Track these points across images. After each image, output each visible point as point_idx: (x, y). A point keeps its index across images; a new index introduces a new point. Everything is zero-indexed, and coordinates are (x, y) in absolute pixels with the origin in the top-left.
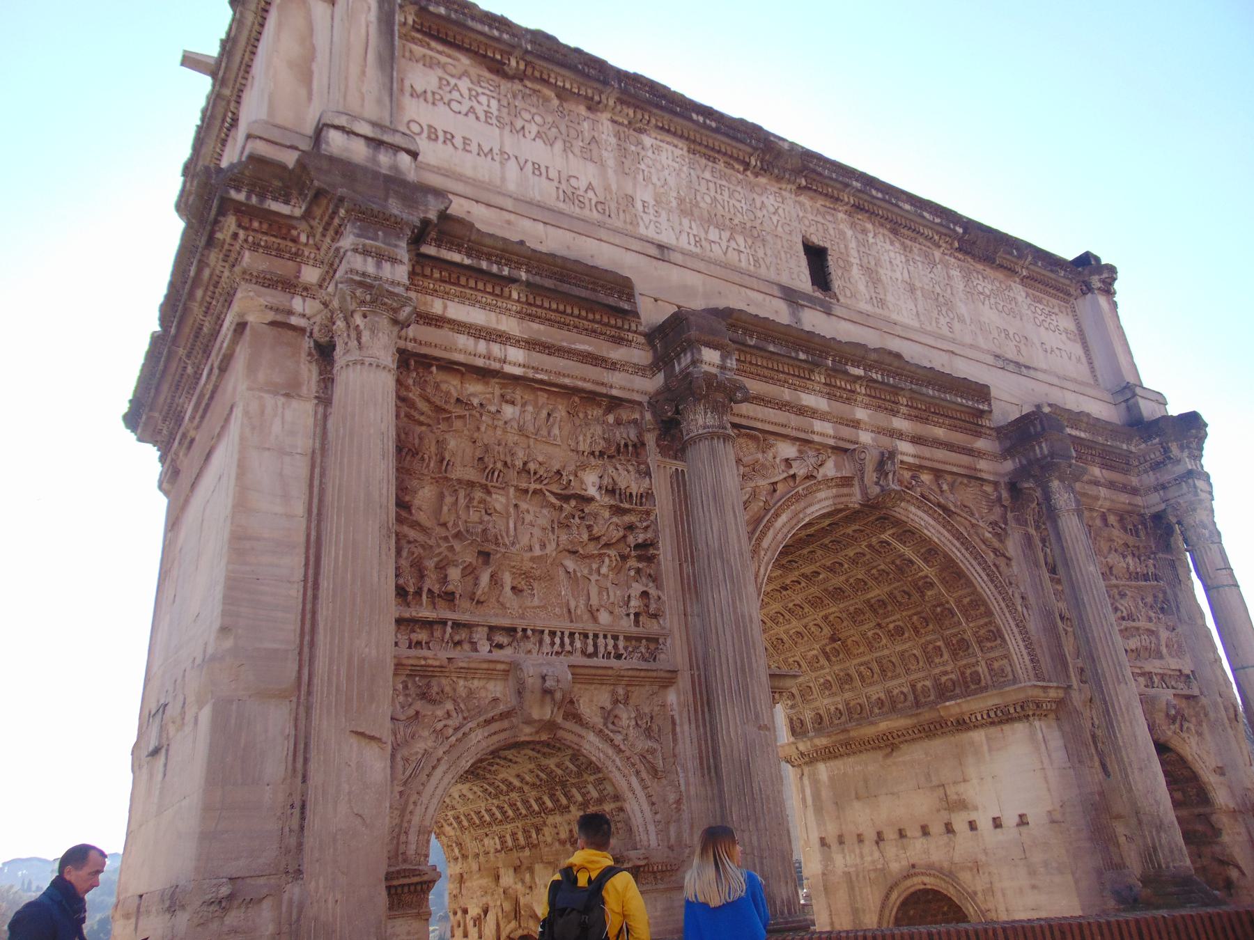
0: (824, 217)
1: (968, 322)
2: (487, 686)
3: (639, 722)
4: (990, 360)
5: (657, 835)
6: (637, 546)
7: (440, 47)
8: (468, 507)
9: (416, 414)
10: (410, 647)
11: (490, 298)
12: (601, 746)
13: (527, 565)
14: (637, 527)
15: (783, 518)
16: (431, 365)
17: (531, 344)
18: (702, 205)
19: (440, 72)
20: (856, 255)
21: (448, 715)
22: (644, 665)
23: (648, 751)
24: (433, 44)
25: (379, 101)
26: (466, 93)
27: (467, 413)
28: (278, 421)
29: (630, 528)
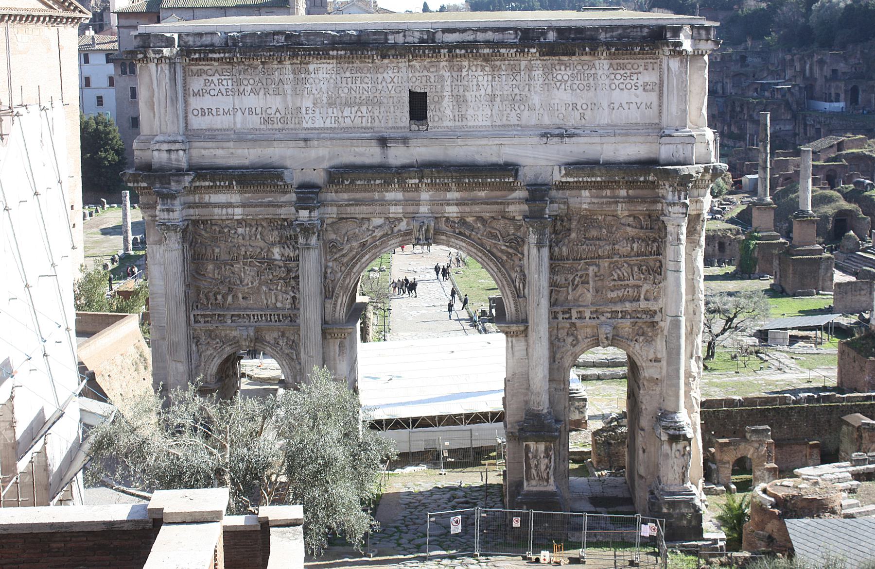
0: (428, 71)
1: (537, 107)
4: (537, 139)
6: (293, 278)
7: (204, 63)
13: (246, 291)
15: (367, 256)
17: (243, 206)
18: (342, 95)
19: (205, 77)
20: (448, 88)
24: (200, 63)
25: (173, 122)
26: (216, 82)
28: (158, 254)
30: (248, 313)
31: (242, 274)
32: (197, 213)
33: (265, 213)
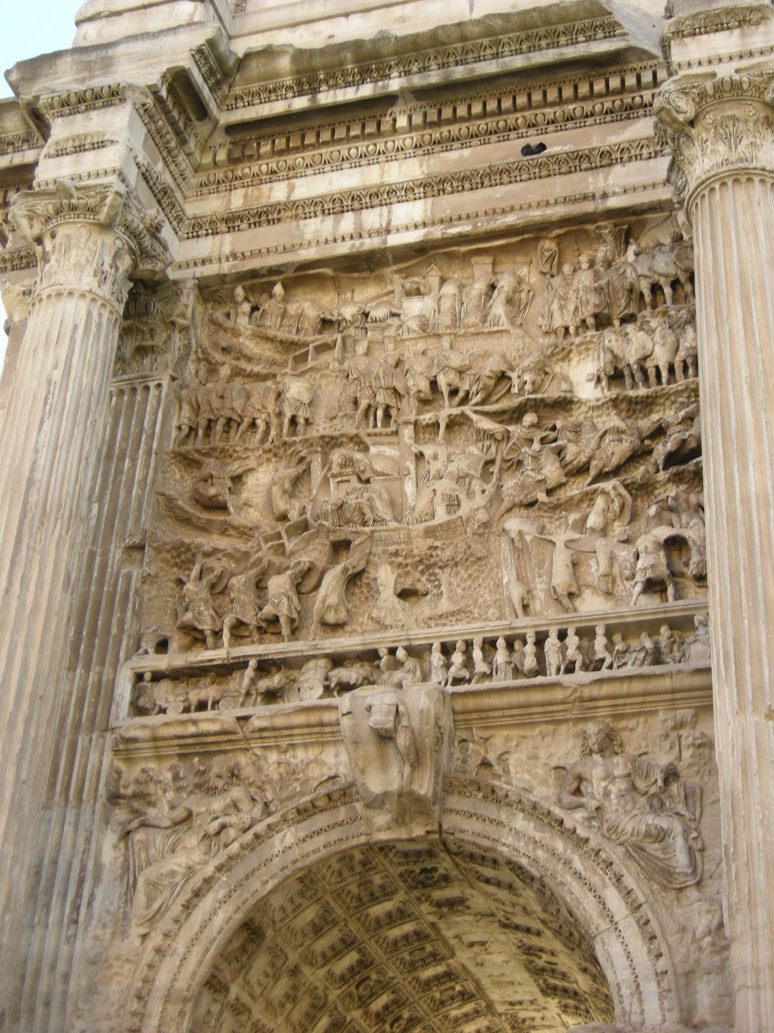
2: (323, 757)
3: (641, 784)
5: (661, 997)
8: (326, 480)
9: (249, 368)
10: (187, 710)
11: (362, 146)
12: (538, 836)
13: (420, 546)
14: (668, 426)
16: (274, 284)
21: (235, 805)
22: (647, 669)
23: (648, 835)
27: (339, 337)
29: (659, 432)
30: (419, 635)
31: (409, 487)
32: (227, 250)
33: (533, 198)
